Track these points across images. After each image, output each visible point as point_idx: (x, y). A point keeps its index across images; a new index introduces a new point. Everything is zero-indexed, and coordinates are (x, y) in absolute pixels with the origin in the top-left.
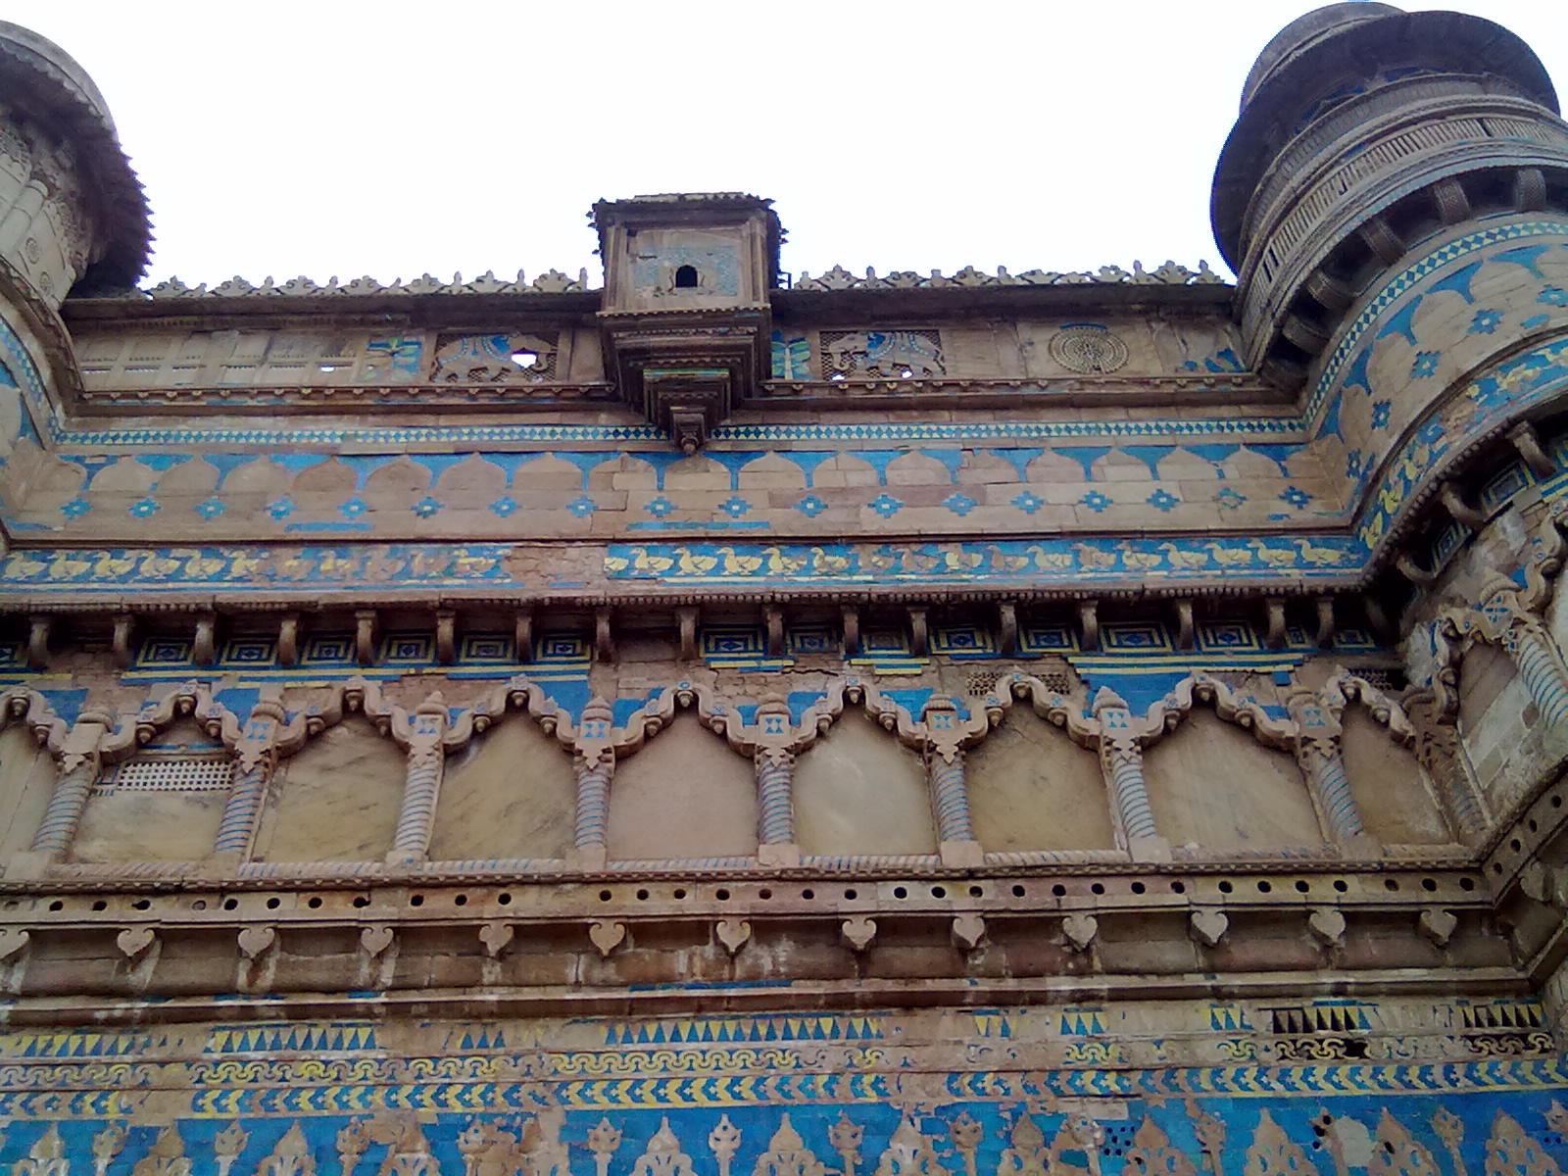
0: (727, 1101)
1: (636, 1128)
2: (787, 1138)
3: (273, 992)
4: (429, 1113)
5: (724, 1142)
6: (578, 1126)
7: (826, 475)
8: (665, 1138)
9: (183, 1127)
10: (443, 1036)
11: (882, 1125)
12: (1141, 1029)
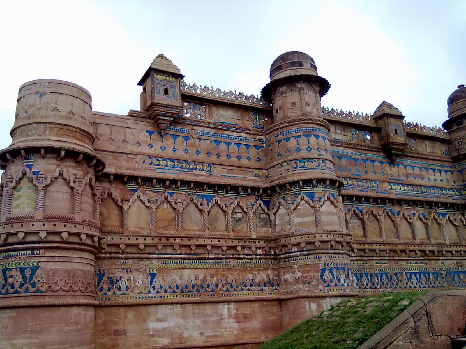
0: (417, 271)
1: (411, 274)
2: (422, 275)
3: (378, 257)
4: (394, 272)
5: (418, 276)
6: (406, 273)
7: (410, 171)
8: (413, 275)
9: (375, 273)
10: (393, 262)
11: (429, 274)
12: (448, 263)
